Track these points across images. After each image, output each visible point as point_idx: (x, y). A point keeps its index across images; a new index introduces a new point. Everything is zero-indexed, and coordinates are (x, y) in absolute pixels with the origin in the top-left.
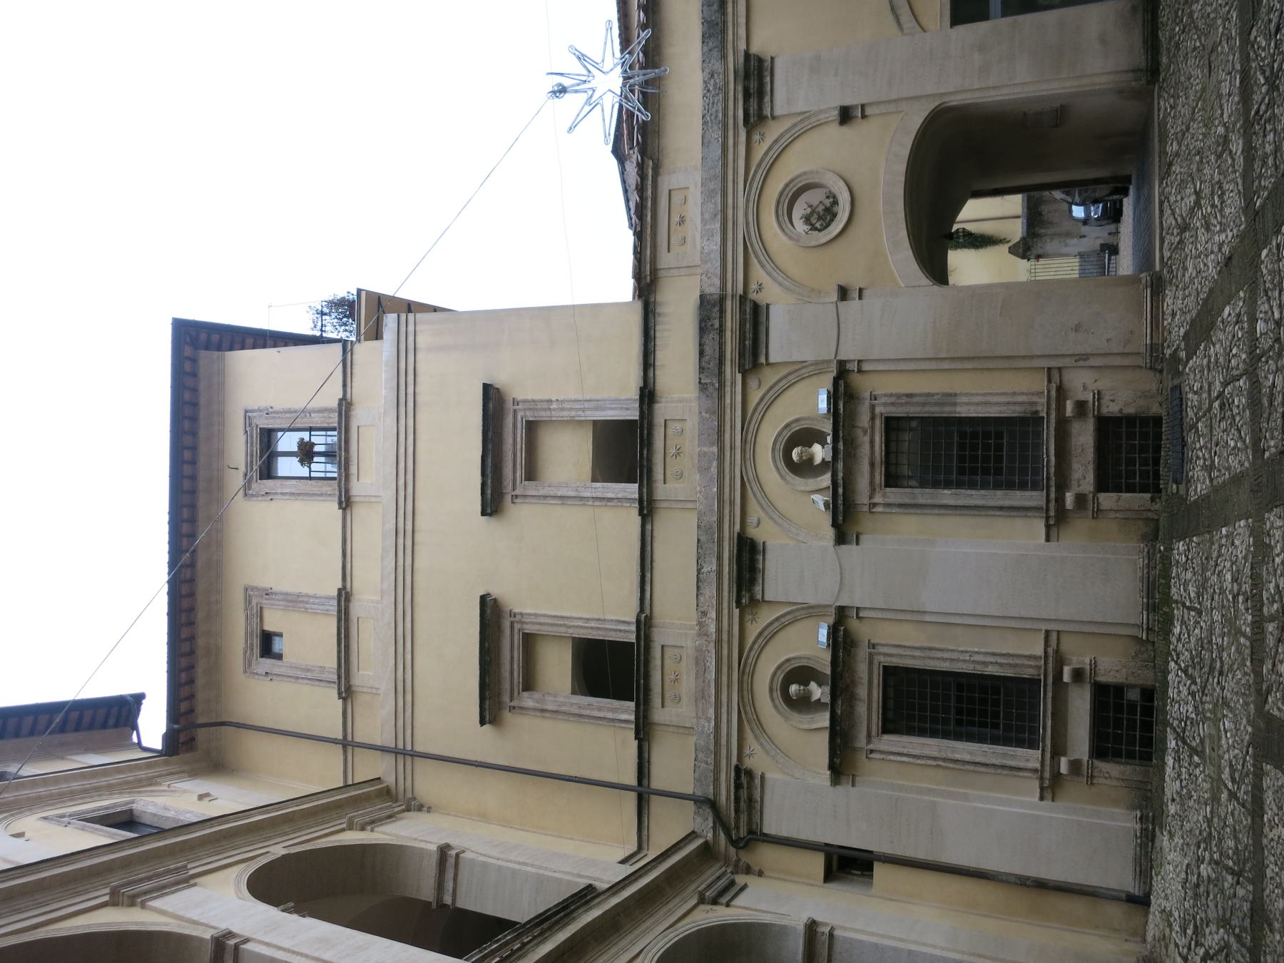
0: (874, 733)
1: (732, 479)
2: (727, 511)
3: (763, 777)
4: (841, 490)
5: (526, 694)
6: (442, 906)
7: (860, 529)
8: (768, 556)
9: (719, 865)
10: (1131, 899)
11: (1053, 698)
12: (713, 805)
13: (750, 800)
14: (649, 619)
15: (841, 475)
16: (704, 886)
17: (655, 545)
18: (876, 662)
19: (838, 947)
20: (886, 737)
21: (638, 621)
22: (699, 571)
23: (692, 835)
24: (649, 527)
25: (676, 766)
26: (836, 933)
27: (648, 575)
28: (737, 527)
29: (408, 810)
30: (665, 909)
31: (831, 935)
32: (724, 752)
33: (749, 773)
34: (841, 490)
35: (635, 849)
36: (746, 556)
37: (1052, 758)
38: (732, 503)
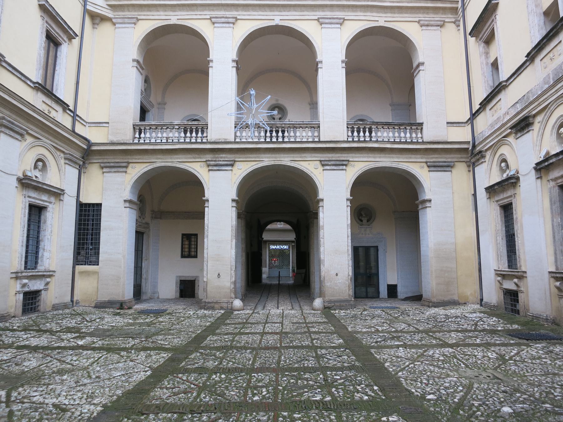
0: (499, 203)
1: (546, 99)
2: (536, 104)
3: (482, 162)
4: (546, 164)
5: (483, 45)
6: (413, 73)
7: (543, 177)
8: (528, 134)
9: (465, 156)
10: (482, 300)
11: (509, 275)
12: (474, 146)
13: (478, 160)
14: (505, 87)
15: (551, 161)
16: (432, 161)
17: (525, 71)
18: (511, 199)
19: (425, 210)
20: (498, 208)
21: (500, 83)
22: (517, 103)
23: (468, 143)
24: (528, 63)
25: (485, 123)
26: (428, 209)
27: (515, 76)
28: (534, 113)
29: (454, 23)
30: (410, 156)
31: (426, 207)
32: (485, 143)
33: (483, 157)
34: (546, 164)
35: (465, 121)
36: (523, 124)
37: (501, 274)
38: (539, 105)
